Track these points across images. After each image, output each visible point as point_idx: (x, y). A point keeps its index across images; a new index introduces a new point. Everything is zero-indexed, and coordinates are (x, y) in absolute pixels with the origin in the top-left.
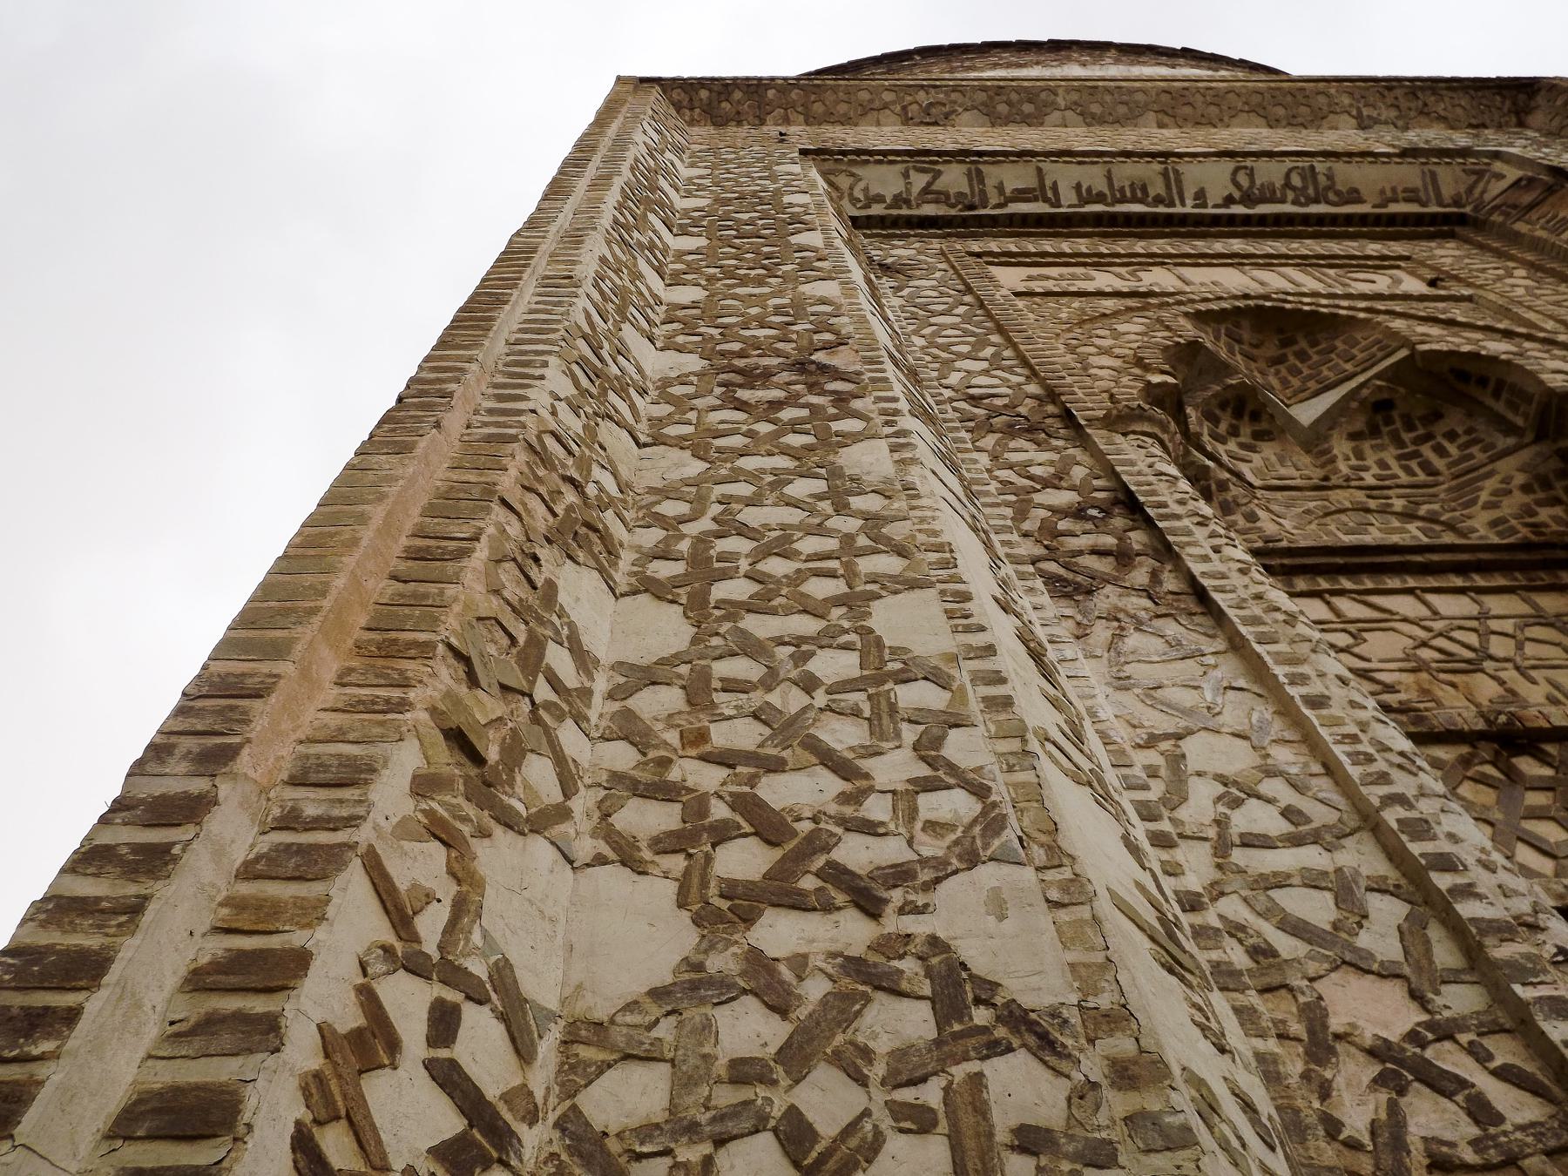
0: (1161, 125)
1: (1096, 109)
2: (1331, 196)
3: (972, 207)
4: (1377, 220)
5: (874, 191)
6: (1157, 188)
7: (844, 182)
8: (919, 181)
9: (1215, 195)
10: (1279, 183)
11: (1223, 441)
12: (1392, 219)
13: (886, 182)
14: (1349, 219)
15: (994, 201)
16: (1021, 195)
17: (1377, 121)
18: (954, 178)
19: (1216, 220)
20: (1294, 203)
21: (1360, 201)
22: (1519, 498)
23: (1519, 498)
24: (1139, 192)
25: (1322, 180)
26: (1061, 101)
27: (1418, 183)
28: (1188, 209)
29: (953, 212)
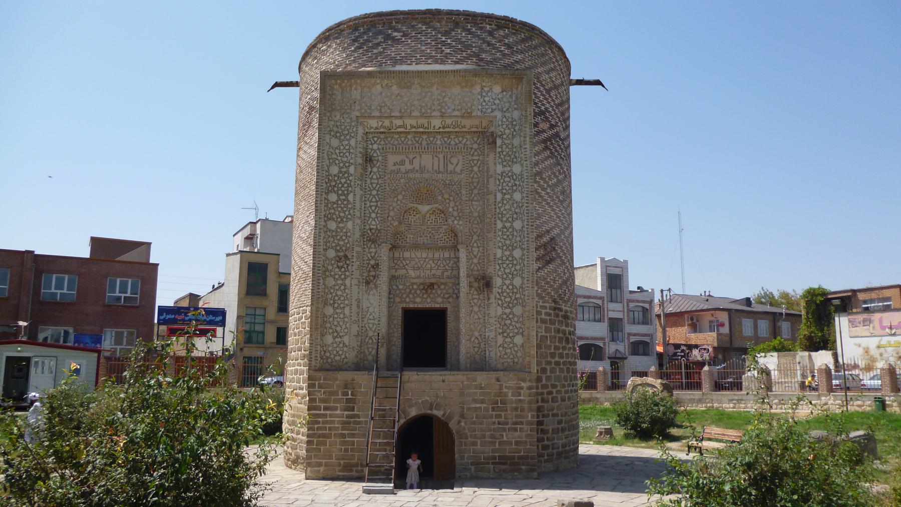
6: (426, 125)
8: (380, 123)
9: (437, 127)
13: (373, 123)
16: (400, 127)
18: (387, 123)
24: (422, 126)
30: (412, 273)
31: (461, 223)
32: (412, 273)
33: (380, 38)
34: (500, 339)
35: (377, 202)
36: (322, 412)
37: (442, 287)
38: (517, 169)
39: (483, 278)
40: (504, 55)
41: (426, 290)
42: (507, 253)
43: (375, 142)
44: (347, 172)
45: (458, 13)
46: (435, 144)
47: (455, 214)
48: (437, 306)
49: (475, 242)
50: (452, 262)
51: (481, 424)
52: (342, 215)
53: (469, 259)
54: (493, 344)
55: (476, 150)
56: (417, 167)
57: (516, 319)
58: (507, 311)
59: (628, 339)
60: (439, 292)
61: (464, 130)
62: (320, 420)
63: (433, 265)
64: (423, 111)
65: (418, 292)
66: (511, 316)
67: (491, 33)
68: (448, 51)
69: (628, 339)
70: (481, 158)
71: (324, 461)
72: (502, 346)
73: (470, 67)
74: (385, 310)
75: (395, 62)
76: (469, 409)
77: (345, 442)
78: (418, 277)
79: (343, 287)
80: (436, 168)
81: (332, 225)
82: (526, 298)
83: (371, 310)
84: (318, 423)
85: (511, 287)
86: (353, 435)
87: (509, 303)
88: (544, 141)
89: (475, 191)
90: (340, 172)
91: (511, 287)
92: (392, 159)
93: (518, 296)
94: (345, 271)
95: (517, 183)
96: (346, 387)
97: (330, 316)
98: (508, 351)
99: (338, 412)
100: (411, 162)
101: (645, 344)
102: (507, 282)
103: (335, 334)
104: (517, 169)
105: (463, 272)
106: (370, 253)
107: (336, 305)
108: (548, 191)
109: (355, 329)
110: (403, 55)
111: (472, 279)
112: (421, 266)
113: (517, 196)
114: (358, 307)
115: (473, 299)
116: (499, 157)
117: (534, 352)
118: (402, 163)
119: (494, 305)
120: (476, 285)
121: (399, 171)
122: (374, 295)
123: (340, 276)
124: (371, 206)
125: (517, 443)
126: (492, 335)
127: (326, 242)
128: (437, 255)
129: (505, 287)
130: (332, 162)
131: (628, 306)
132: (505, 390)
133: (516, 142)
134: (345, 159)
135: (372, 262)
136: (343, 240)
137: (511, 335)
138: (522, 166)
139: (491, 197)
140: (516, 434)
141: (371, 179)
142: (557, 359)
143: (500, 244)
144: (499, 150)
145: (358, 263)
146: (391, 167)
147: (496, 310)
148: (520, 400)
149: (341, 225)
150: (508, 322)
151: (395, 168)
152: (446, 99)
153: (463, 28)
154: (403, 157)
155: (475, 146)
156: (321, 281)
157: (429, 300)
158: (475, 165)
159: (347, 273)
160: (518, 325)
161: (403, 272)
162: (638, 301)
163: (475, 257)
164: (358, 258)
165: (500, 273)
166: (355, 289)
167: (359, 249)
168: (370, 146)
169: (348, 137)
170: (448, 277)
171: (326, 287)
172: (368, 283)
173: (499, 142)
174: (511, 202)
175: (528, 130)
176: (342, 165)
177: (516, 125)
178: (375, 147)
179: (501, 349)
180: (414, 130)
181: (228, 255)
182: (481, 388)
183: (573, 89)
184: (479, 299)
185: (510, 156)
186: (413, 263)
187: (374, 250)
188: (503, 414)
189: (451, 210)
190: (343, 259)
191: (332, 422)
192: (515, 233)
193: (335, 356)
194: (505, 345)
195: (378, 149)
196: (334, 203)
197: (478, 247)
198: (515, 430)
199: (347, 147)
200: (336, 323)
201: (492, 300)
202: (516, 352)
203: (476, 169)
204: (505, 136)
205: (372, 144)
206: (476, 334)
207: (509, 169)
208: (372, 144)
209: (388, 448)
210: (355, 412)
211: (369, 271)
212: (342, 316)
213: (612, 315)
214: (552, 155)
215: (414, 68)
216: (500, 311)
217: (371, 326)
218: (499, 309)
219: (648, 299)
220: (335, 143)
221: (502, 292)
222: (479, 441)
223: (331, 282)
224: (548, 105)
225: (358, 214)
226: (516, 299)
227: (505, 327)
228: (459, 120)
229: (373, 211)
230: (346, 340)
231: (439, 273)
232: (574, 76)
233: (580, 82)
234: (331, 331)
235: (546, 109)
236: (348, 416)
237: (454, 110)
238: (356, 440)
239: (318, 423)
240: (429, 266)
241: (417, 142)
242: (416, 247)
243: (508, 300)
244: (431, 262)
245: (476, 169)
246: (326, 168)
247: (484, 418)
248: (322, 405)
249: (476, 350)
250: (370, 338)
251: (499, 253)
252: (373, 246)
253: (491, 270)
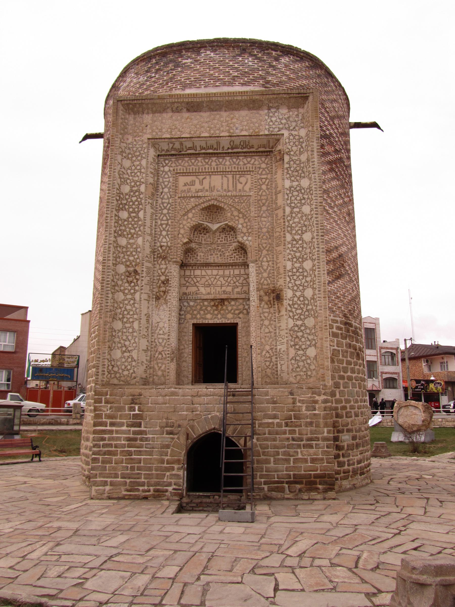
0: (225, 111)
1: (212, 107)
2: (248, 147)
3: (180, 152)
4: (257, 152)
5: (163, 148)
6: (215, 146)
7: (157, 146)
8: (171, 145)
9: (226, 148)
10: (239, 144)
11: (201, 234)
12: (259, 152)
13: (165, 146)
14: (251, 152)
15: (185, 150)
16: (190, 148)
17: (272, 107)
18: (177, 146)
19: (226, 153)
20: (241, 148)
21: (253, 148)
22: (233, 252)
23: (233, 252)
24: (212, 147)
25: (247, 143)
26: (205, 105)
27: (266, 143)
28: (221, 151)
29: (177, 153)
30: (202, 290)
31: (250, 238)
32: (202, 290)
33: (171, 66)
34: (292, 352)
35: (167, 220)
36: (108, 428)
37: (233, 303)
38: (305, 183)
39: (273, 291)
40: (290, 79)
41: (217, 306)
42: (297, 265)
43: (167, 165)
44: (138, 191)
45: (244, 41)
46: (224, 165)
47: (245, 230)
48: (229, 322)
49: (265, 256)
50: (242, 279)
51: (275, 440)
52: (133, 231)
53: (258, 274)
54: (285, 357)
55: (264, 169)
56: (207, 187)
57: (308, 331)
58: (299, 323)
59: (382, 376)
60: (230, 308)
61: (252, 150)
62: (106, 436)
63: (224, 282)
64: (212, 132)
65: (209, 308)
66: (303, 328)
67: (277, 59)
68: (236, 74)
69: (382, 376)
70: (269, 176)
71: (109, 480)
72: (294, 358)
73: (257, 89)
74: (175, 325)
75: (185, 87)
76: (260, 425)
77: (131, 459)
78: (208, 294)
79: (132, 302)
80: (225, 187)
81: (123, 241)
82: (318, 308)
83: (161, 325)
84: (103, 439)
85: (302, 299)
86: (140, 453)
87: (301, 314)
88: (330, 163)
89: (264, 208)
90: (131, 191)
91: (302, 299)
92: (182, 180)
93: (310, 307)
94: (135, 286)
95: (306, 197)
96: (133, 402)
97: (119, 331)
98: (301, 364)
99: (124, 428)
100: (201, 183)
101: (394, 380)
102: (298, 294)
103: (124, 349)
104: (305, 183)
105: (253, 286)
106: (161, 269)
107: (125, 320)
108: (336, 209)
109: (144, 344)
110: (192, 79)
111: (262, 293)
112: (211, 283)
113: (306, 209)
114: (148, 321)
115: (264, 313)
116: (288, 173)
117: (328, 363)
118: (193, 183)
119: (286, 317)
120: (266, 298)
121: (189, 190)
122: (164, 310)
123: (129, 291)
124: (161, 225)
125: (313, 460)
126: (284, 347)
127: (116, 258)
128: (227, 272)
129: (296, 299)
130: (124, 181)
131: (380, 351)
132: (298, 404)
133: (304, 158)
134: (137, 179)
135: (163, 278)
136: (133, 256)
137: (303, 347)
138: (310, 179)
139: (280, 212)
140: (312, 451)
141: (162, 199)
142: (349, 374)
143: (290, 257)
144: (286, 166)
145: (148, 278)
146: (181, 187)
147: (287, 323)
148: (315, 414)
149: (131, 241)
150: (300, 334)
151: (186, 188)
152: (234, 120)
153: (250, 53)
154: (194, 178)
155: (263, 166)
156: (110, 295)
157: (219, 316)
158: (264, 183)
159: (137, 288)
160: (310, 337)
161: (194, 289)
162: (387, 348)
163: (265, 271)
164: (148, 273)
165: (290, 285)
166: (144, 304)
167: (150, 265)
168: (162, 169)
169: (139, 158)
170: (238, 293)
171: (115, 301)
172: (158, 298)
173: (286, 158)
174: (299, 215)
175: (315, 145)
176: (133, 184)
177: (302, 142)
178: (167, 169)
179: (293, 362)
180: (203, 151)
181: (82, 314)
182: (275, 402)
183: (353, 132)
184: (269, 313)
185: (297, 171)
186: (203, 280)
187: (164, 266)
188: (297, 429)
189: (240, 226)
190: (133, 274)
191: (119, 439)
192: (305, 245)
193: (123, 370)
194: (298, 358)
195: (170, 170)
196: (125, 220)
197: (268, 262)
198: (311, 446)
199: (138, 168)
200: (124, 338)
201: (283, 312)
202: (309, 364)
203: (264, 187)
204: (292, 153)
205: (163, 167)
206: (268, 348)
207: (296, 183)
208: (163, 167)
209: (176, 466)
210: (143, 428)
211: (160, 287)
212: (131, 330)
213: (369, 358)
214: (337, 178)
215: (203, 91)
216: (291, 323)
217: (161, 341)
218: (290, 320)
219: (395, 347)
220: (127, 163)
221: (293, 304)
222: (272, 459)
223: (120, 296)
224: (332, 131)
225: (148, 230)
226: (307, 310)
227: (297, 340)
228: (247, 141)
229: (164, 229)
230: (134, 354)
231: (229, 289)
232: (353, 119)
233: (358, 125)
234: (120, 345)
235: (331, 134)
236: (135, 433)
237: (242, 130)
238: (143, 457)
239: (103, 439)
240: (219, 283)
241: (207, 163)
242: (207, 265)
243: (299, 311)
244: (221, 279)
245: (264, 187)
246: (117, 186)
247: (277, 434)
248: (108, 421)
249: (268, 363)
250: (160, 353)
251: (289, 265)
252: (163, 262)
253: (281, 282)
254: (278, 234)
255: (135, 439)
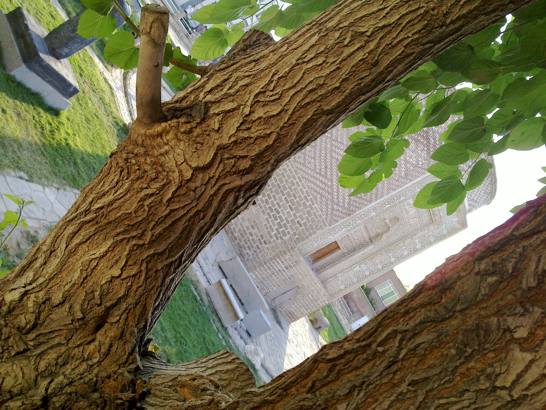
84: (274, 263)
100: (410, 207)
155: (424, 222)
203: (413, 228)
236: (283, 270)
254: (391, 248)
255: (280, 271)
